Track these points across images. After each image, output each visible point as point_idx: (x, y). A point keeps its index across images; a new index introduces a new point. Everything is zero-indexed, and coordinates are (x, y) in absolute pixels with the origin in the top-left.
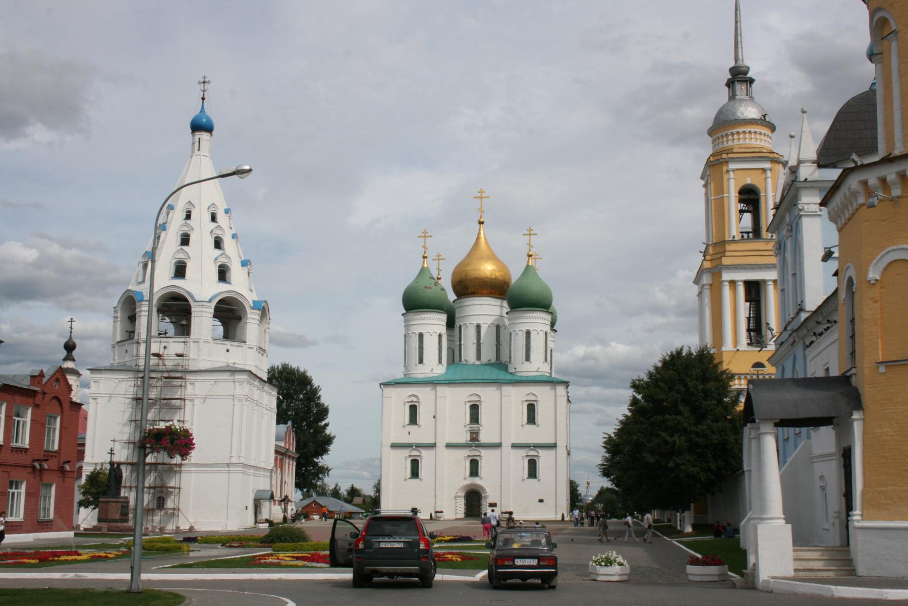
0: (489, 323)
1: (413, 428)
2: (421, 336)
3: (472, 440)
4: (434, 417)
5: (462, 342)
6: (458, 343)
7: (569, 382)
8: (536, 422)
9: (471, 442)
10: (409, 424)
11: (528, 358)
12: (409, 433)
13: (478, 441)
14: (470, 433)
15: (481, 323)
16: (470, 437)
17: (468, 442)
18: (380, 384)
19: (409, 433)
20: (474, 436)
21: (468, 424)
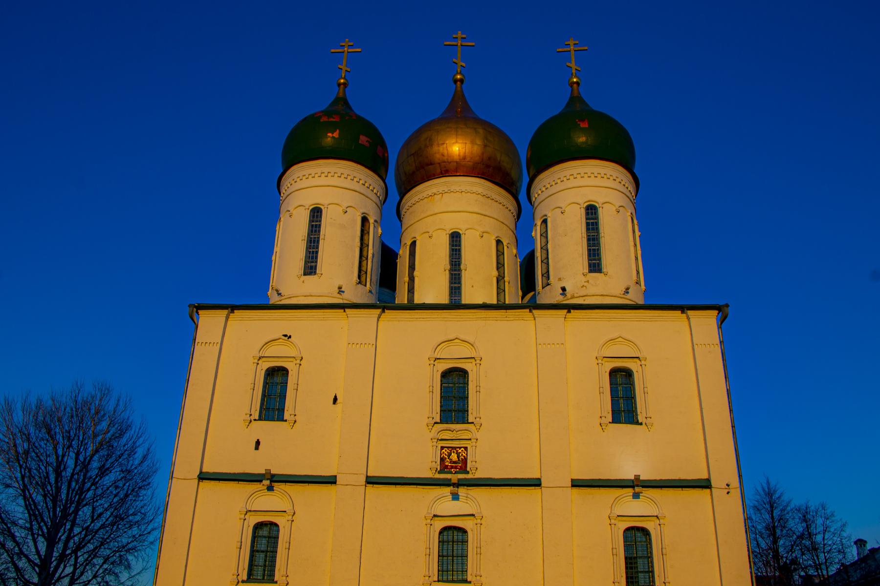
0: (482, 230)
1: (267, 429)
2: (316, 213)
3: (444, 469)
4: (335, 400)
5: (415, 273)
6: (407, 279)
7: (727, 306)
8: (641, 419)
9: (442, 476)
10: (260, 419)
11: (595, 265)
12: (258, 443)
13: (468, 473)
14: (442, 448)
15: (461, 227)
16: (441, 459)
17: (438, 476)
18: (190, 306)
19: (258, 443)
20: (454, 457)
21: (436, 423)
